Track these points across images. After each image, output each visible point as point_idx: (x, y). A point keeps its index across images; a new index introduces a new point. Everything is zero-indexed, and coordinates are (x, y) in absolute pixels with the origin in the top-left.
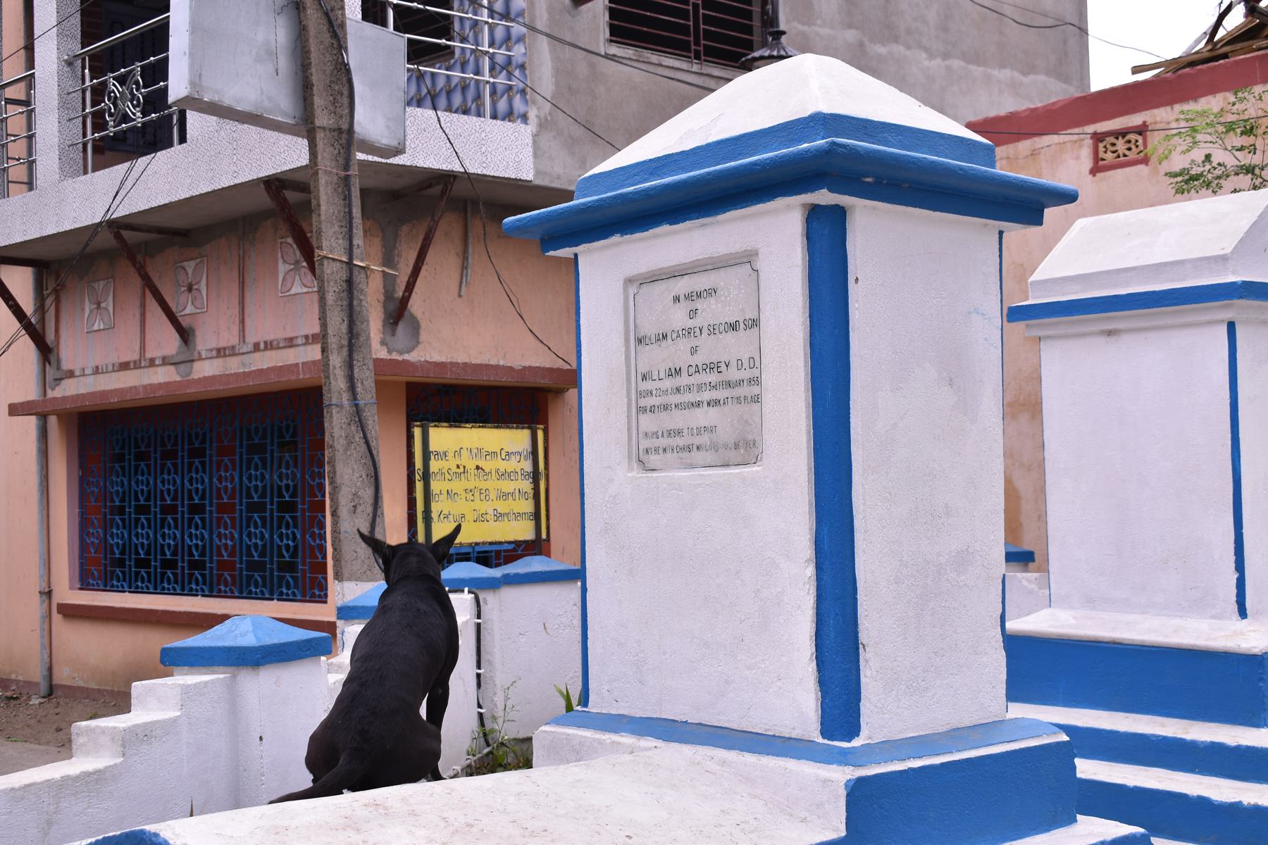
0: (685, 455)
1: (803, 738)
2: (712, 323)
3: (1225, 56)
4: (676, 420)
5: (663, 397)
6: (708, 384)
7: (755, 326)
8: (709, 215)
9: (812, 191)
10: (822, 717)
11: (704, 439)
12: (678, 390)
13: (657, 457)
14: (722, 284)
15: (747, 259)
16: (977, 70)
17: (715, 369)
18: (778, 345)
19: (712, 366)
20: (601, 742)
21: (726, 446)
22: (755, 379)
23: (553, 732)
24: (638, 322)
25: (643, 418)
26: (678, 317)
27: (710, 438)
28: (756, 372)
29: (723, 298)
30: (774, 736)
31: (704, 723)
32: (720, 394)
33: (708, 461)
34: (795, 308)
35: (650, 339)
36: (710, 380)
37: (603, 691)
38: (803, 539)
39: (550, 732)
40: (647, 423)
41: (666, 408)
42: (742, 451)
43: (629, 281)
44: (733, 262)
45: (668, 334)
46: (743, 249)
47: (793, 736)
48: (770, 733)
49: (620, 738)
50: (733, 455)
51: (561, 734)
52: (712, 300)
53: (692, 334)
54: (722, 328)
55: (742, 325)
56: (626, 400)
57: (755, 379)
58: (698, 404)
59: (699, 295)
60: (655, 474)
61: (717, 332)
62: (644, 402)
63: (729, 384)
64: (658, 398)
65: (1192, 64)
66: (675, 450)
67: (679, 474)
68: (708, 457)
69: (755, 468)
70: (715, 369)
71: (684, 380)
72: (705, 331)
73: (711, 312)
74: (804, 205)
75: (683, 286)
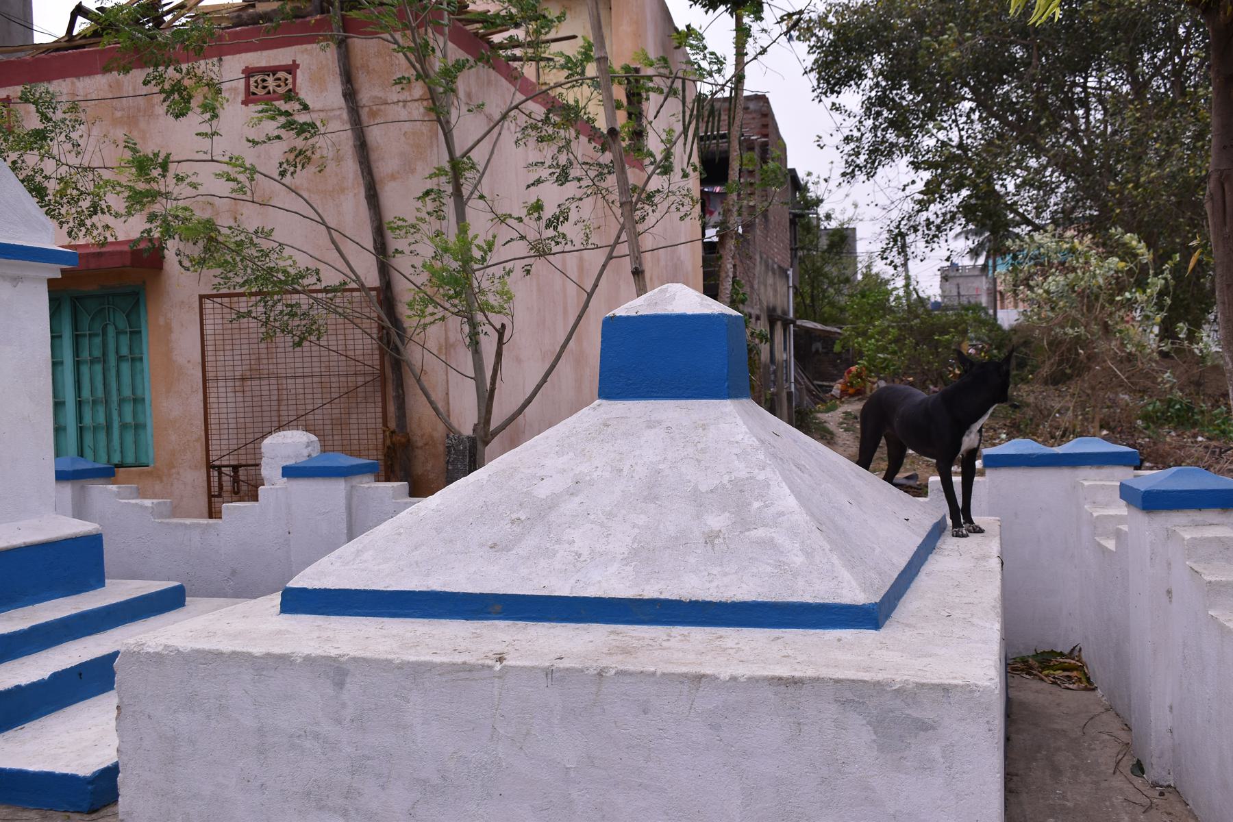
3: (83, 46)
65: (57, 50)
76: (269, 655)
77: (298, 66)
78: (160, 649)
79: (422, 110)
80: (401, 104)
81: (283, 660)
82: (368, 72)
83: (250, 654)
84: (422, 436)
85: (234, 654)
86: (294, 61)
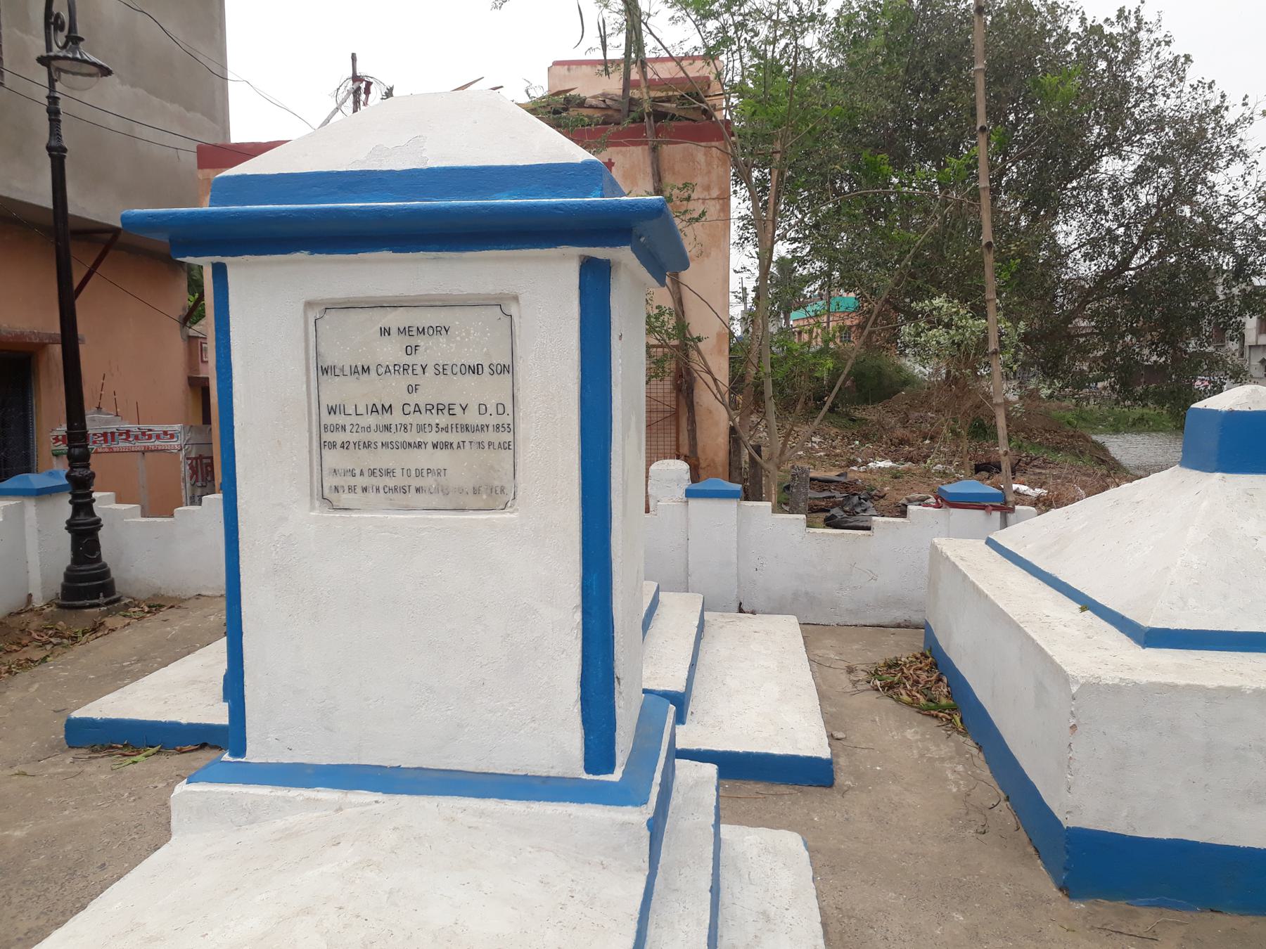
0: (398, 497)
1: (565, 776)
2: (441, 363)
4: (385, 459)
5: (362, 434)
6: (434, 426)
7: (506, 372)
8: (458, 250)
9: (613, 245)
10: (586, 753)
11: (429, 481)
12: (387, 428)
13: (352, 495)
14: (457, 323)
15: (500, 303)
16: (155, 101)
17: (446, 411)
18: (545, 395)
19: (441, 407)
20: (287, 801)
21: (461, 491)
22: (506, 426)
23: (206, 792)
24: (321, 350)
25: (326, 452)
26: (391, 351)
27: (436, 481)
28: (509, 420)
29: (458, 338)
30: (526, 775)
31: (424, 767)
32: (453, 437)
33: (434, 504)
34: (569, 360)
35: (342, 370)
36: (437, 421)
37: (269, 739)
38: (572, 585)
39: (201, 792)
40: (333, 458)
41: (367, 445)
42: (485, 497)
43: (309, 305)
44: (476, 303)
45: (371, 368)
46: (498, 292)
47: (552, 774)
48: (520, 773)
49: (316, 793)
50: (471, 500)
51: (221, 793)
52: (442, 339)
53: (410, 371)
54: (456, 370)
55: (486, 369)
56: (307, 435)
57: (506, 426)
58: (419, 445)
59: (421, 331)
60: (355, 515)
61: (449, 372)
62: (328, 437)
63: (466, 428)
64: (355, 434)
66: (382, 491)
67: (393, 516)
68: (435, 500)
69: (506, 516)
70: (446, 411)
71: (396, 418)
72: (430, 371)
73: (433, 351)
74: (580, 256)
75: (395, 319)
76: (1221, 688)
77: (613, 164)
78: (1117, 681)
79: (718, 207)
80: (701, 201)
81: (1235, 692)
82: (674, 173)
83: (1204, 686)
84: (706, 459)
85: (1189, 688)
86: (610, 160)
